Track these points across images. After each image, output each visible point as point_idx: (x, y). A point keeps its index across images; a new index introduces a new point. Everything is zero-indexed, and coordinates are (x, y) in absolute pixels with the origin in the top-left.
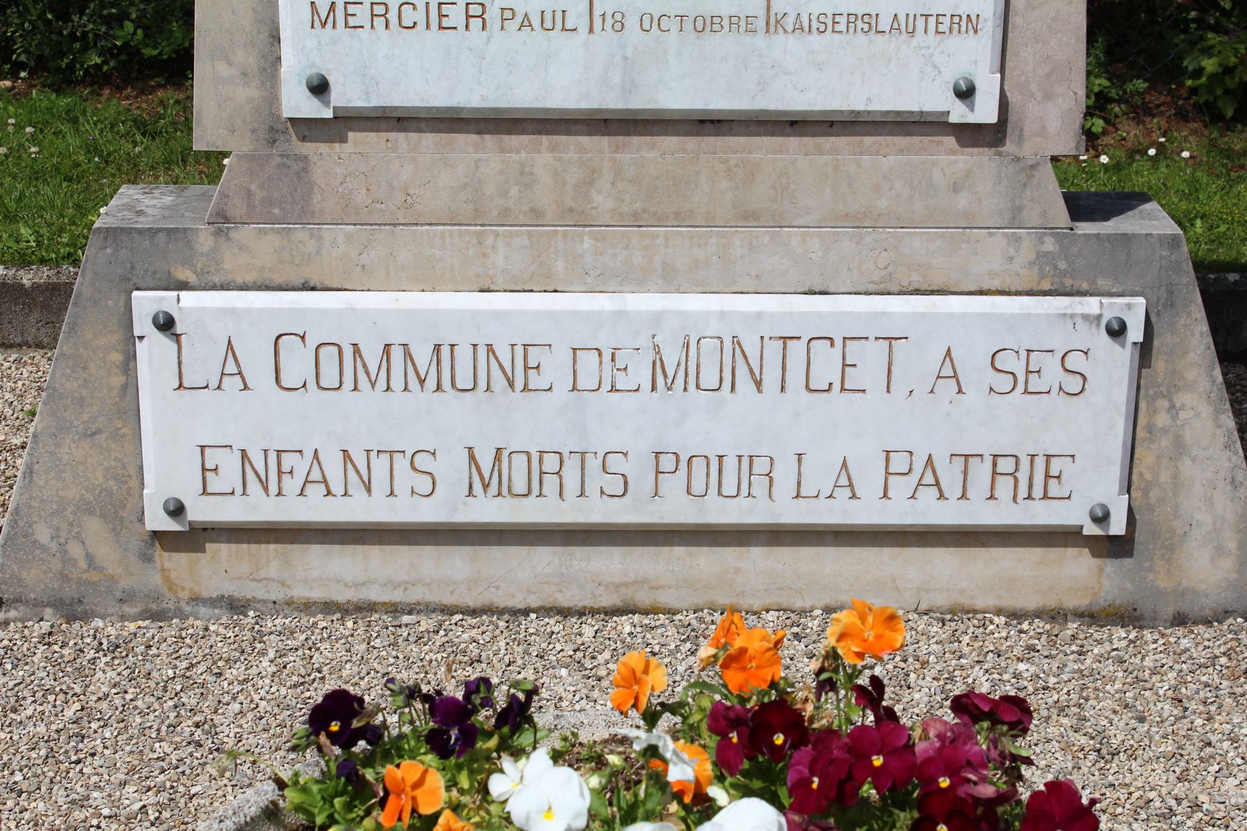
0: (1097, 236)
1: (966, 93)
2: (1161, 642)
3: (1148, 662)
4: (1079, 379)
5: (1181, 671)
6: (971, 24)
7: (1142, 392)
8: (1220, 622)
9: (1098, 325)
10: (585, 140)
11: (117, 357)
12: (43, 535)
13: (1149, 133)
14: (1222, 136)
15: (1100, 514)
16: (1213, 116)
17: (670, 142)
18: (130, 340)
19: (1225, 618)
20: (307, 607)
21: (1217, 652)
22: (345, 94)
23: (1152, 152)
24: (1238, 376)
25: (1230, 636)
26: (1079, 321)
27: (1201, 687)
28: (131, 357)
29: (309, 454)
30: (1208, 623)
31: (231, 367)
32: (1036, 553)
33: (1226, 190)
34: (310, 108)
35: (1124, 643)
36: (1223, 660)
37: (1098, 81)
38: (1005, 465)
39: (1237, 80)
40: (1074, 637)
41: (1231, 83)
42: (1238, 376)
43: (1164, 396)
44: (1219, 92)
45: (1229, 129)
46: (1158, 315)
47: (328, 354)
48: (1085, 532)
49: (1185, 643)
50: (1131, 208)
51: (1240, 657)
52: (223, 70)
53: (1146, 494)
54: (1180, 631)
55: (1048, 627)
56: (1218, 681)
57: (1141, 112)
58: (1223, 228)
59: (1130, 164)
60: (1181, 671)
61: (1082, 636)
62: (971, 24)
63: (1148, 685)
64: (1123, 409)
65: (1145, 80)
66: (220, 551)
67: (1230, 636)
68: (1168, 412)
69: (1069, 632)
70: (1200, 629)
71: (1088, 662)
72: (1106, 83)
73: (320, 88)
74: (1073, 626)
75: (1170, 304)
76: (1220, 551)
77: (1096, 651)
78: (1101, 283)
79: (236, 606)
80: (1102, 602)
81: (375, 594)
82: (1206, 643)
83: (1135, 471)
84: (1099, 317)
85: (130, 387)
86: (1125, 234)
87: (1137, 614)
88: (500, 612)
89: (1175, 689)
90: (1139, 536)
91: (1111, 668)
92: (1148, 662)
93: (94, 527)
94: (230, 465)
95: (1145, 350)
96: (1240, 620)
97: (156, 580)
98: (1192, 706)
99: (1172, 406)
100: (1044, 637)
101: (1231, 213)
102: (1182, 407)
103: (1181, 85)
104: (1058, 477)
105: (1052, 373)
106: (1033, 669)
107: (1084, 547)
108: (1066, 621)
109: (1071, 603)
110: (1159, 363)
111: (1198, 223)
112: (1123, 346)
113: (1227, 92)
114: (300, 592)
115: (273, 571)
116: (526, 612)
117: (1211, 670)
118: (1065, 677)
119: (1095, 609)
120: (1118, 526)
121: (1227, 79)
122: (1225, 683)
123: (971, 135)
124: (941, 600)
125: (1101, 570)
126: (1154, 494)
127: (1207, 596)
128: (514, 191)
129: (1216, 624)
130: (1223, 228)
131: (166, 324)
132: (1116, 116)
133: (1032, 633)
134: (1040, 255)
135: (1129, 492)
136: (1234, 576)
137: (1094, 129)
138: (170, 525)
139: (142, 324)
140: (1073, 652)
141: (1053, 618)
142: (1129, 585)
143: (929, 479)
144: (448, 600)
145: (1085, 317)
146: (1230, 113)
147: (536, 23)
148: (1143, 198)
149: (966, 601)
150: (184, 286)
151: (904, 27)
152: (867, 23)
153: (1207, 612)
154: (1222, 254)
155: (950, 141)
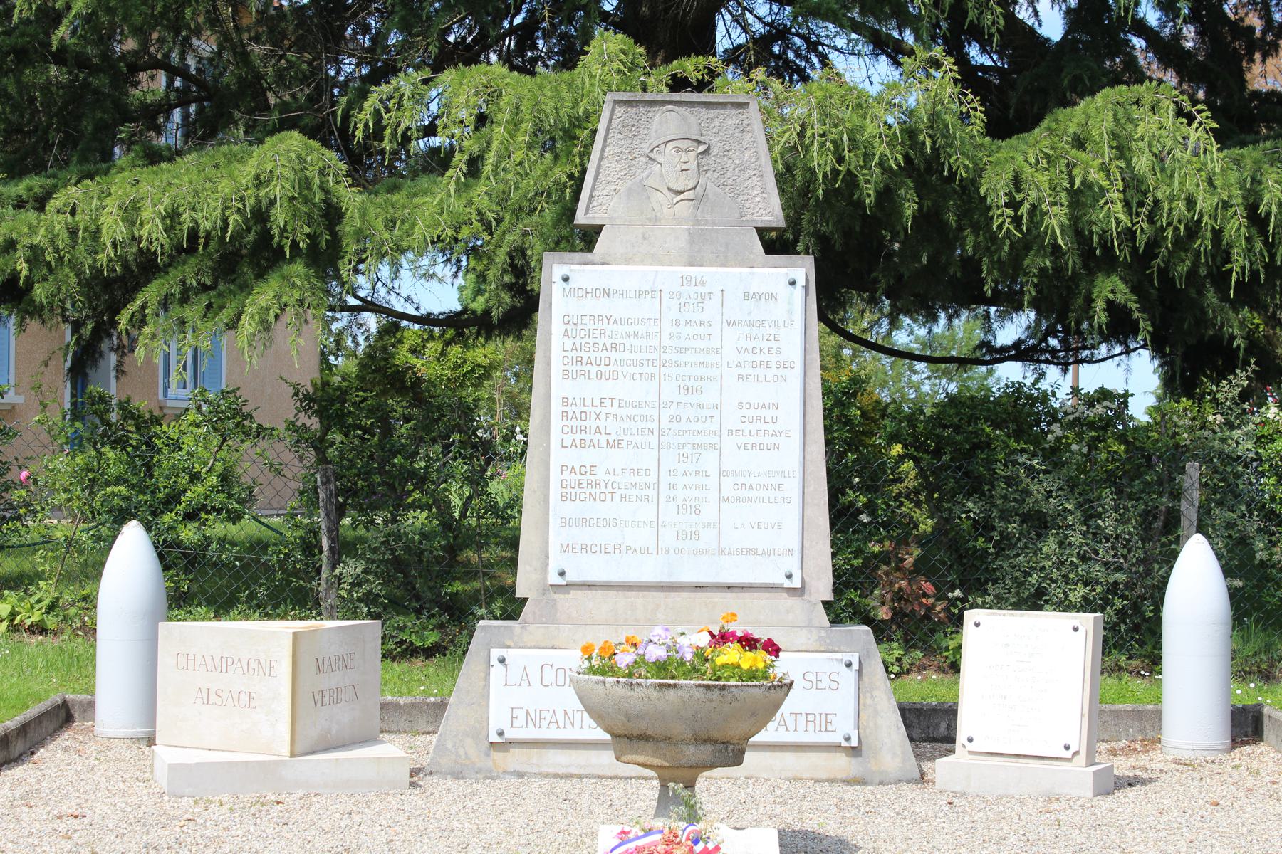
1: (789, 576)
6: (790, 552)
10: (655, 593)
11: (483, 675)
12: (449, 745)
17: (685, 594)
18: (489, 665)
20: (547, 775)
22: (571, 576)
28: (488, 674)
29: (551, 711)
31: (525, 677)
32: (824, 755)
34: (559, 581)
38: (811, 718)
47: (561, 672)
52: (528, 568)
53: (865, 730)
62: (790, 552)
66: (515, 752)
73: (562, 574)
79: (520, 775)
81: (574, 771)
85: (487, 686)
88: (621, 778)
93: (469, 741)
94: (521, 715)
97: (490, 764)
105: (826, 682)
109: (839, 777)
110: (866, 679)
114: (545, 770)
115: (535, 761)
116: (631, 778)
120: (854, 743)
123: (792, 591)
124: (790, 775)
126: (868, 731)
128: (629, 612)
131: (502, 661)
134: (819, 637)
138: (499, 740)
139: (494, 661)
143: (782, 723)
144: (601, 773)
147: (638, 551)
149: (799, 775)
150: (509, 647)
151: (767, 553)
152: (753, 551)
155: (785, 595)
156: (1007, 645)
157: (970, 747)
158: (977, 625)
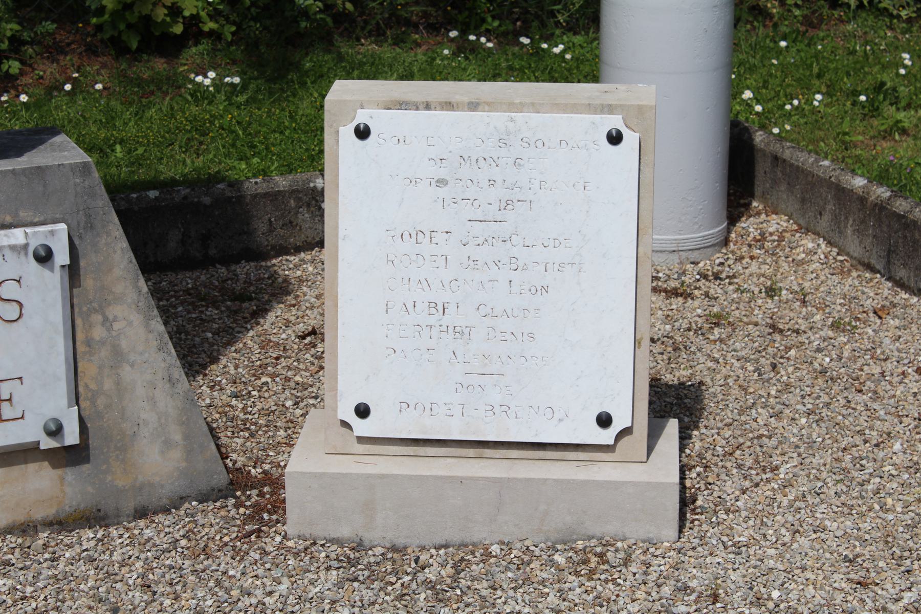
0: (13, 172)
2: (126, 536)
3: (116, 556)
4: (16, 306)
5: (147, 559)
7: (76, 310)
8: (177, 508)
9: (26, 254)
13: (64, 70)
14: (130, 67)
15: (53, 427)
16: (119, 49)
19: (182, 504)
21: (177, 536)
23: (68, 87)
24: (171, 282)
25: (187, 519)
26: (8, 253)
27: (166, 570)
30: (166, 511)
33: (139, 115)
35: (92, 543)
36: (184, 542)
37: (10, 26)
39: (137, 14)
40: (46, 546)
41: (132, 18)
42: (171, 282)
43: (96, 311)
44: (122, 27)
45: (136, 60)
46: (80, 237)
48: (42, 447)
49: (148, 533)
50: (42, 142)
51: (198, 537)
54: (142, 523)
55: (20, 541)
56: (180, 562)
57: (54, 51)
58: (140, 151)
59: (50, 100)
60: (147, 559)
61: (53, 544)
63: (118, 578)
64: (61, 328)
65: (53, 21)
67: (187, 519)
68: (103, 325)
69: (41, 542)
70: (161, 517)
71: (61, 566)
72: (16, 27)
74: (44, 535)
75: (90, 226)
76: (168, 444)
77: (67, 555)
78: (23, 215)
80: (67, 508)
82: (167, 530)
83: (81, 383)
84: (26, 246)
86: (39, 167)
87: (101, 514)
89: (143, 576)
90: (93, 442)
91: (83, 568)
92: (116, 556)
95: (73, 271)
96: (194, 503)
98: (160, 589)
99: (106, 319)
100: (17, 550)
101: (146, 136)
102: (115, 319)
103: (86, 23)
104: (10, 400)
106: (9, 582)
107: (43, 460)
108: (36, 532)
109: (39, 514)
110: (88, 282)
111: (118, 148)
112: (52, 269)
113: (129, 26)
117: (173, 553)
118: (41, 584)
119: (62, 516)
120: (72, 437)
121: (127, 14)
122: (187, 563)
125: (62, 479)
126: (101, 402)
127: (162, 486)
129: (173, 511)
130: (140, 151)
132: (31, 57)
133: (5, 549)
135: (77, 403)
136: (184, 464)
137: (11, 71)
140: (46, 560)
141: (24, 531)
142: (90, 489)
145: (13, 248)
146: (134, 45)
148: (53, 131)
153: (165, 501)
154: (142, 174)
156: (441, 182)
157: (362, 427)
158: (363, 133)
